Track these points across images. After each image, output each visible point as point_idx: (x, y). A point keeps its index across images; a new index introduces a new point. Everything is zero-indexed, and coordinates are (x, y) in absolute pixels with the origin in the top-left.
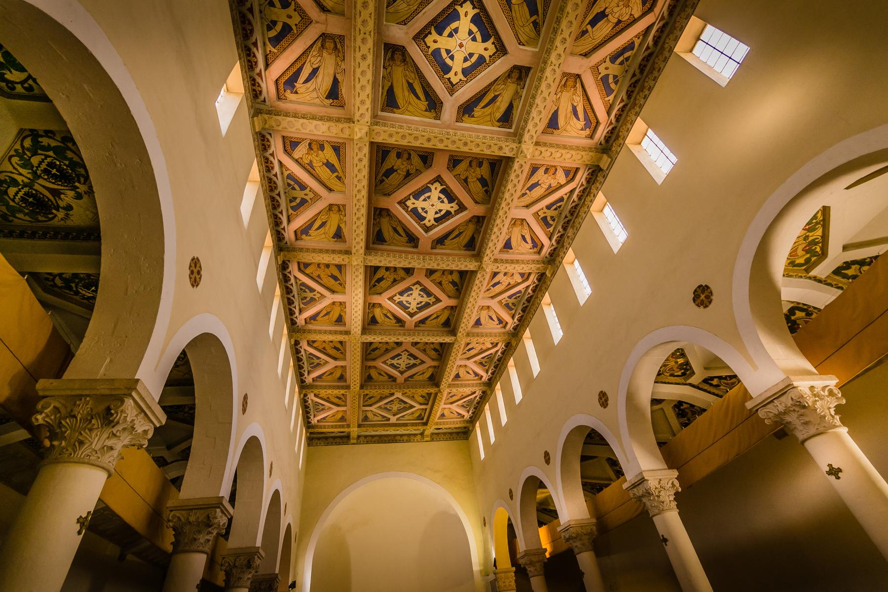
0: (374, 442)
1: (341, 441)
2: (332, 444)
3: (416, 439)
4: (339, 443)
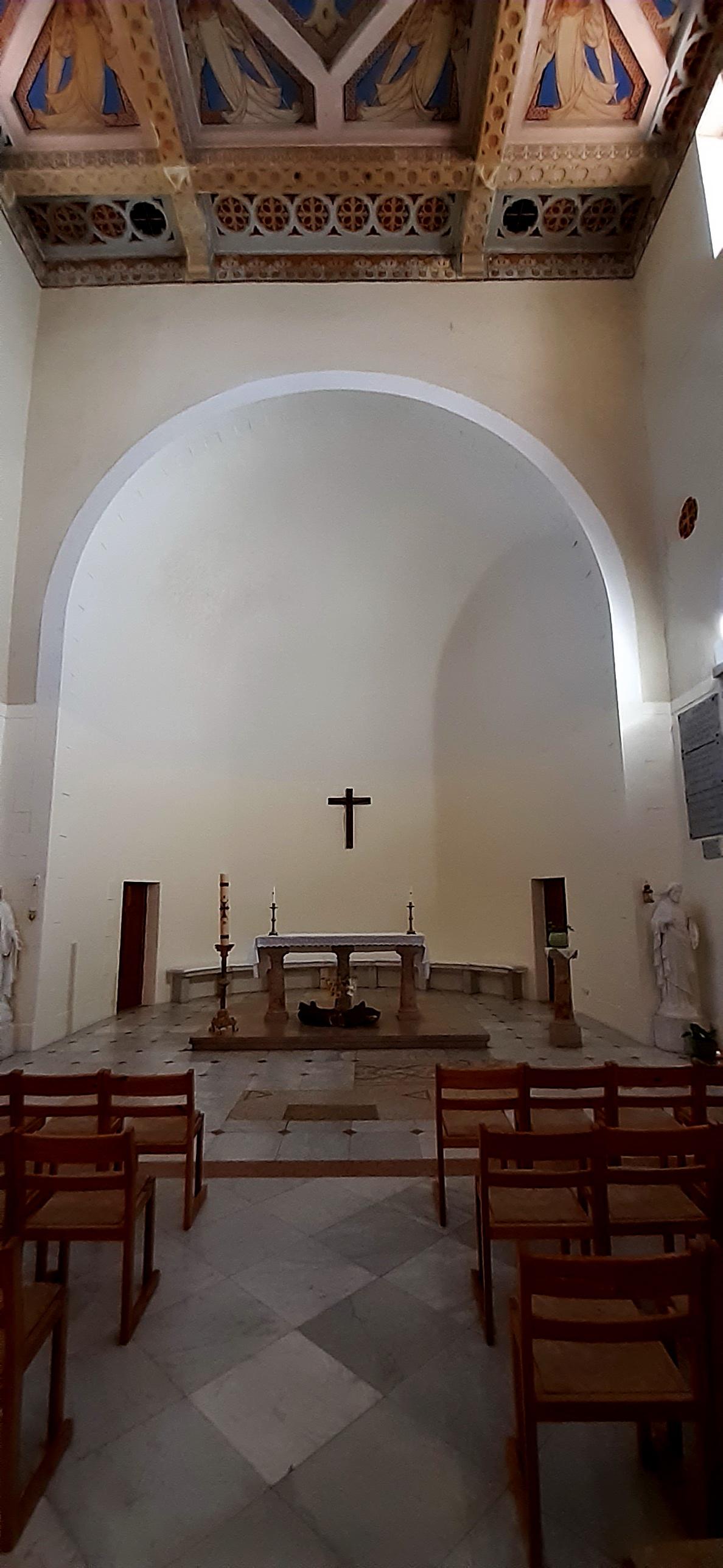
0: (276, 278)
1: (156, 271)
2: (124, 282)
3: (428, 271)
4: (152, 277)
